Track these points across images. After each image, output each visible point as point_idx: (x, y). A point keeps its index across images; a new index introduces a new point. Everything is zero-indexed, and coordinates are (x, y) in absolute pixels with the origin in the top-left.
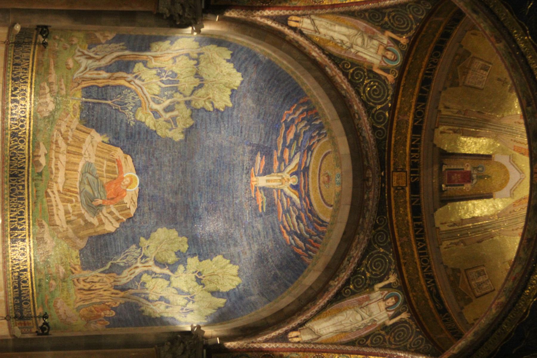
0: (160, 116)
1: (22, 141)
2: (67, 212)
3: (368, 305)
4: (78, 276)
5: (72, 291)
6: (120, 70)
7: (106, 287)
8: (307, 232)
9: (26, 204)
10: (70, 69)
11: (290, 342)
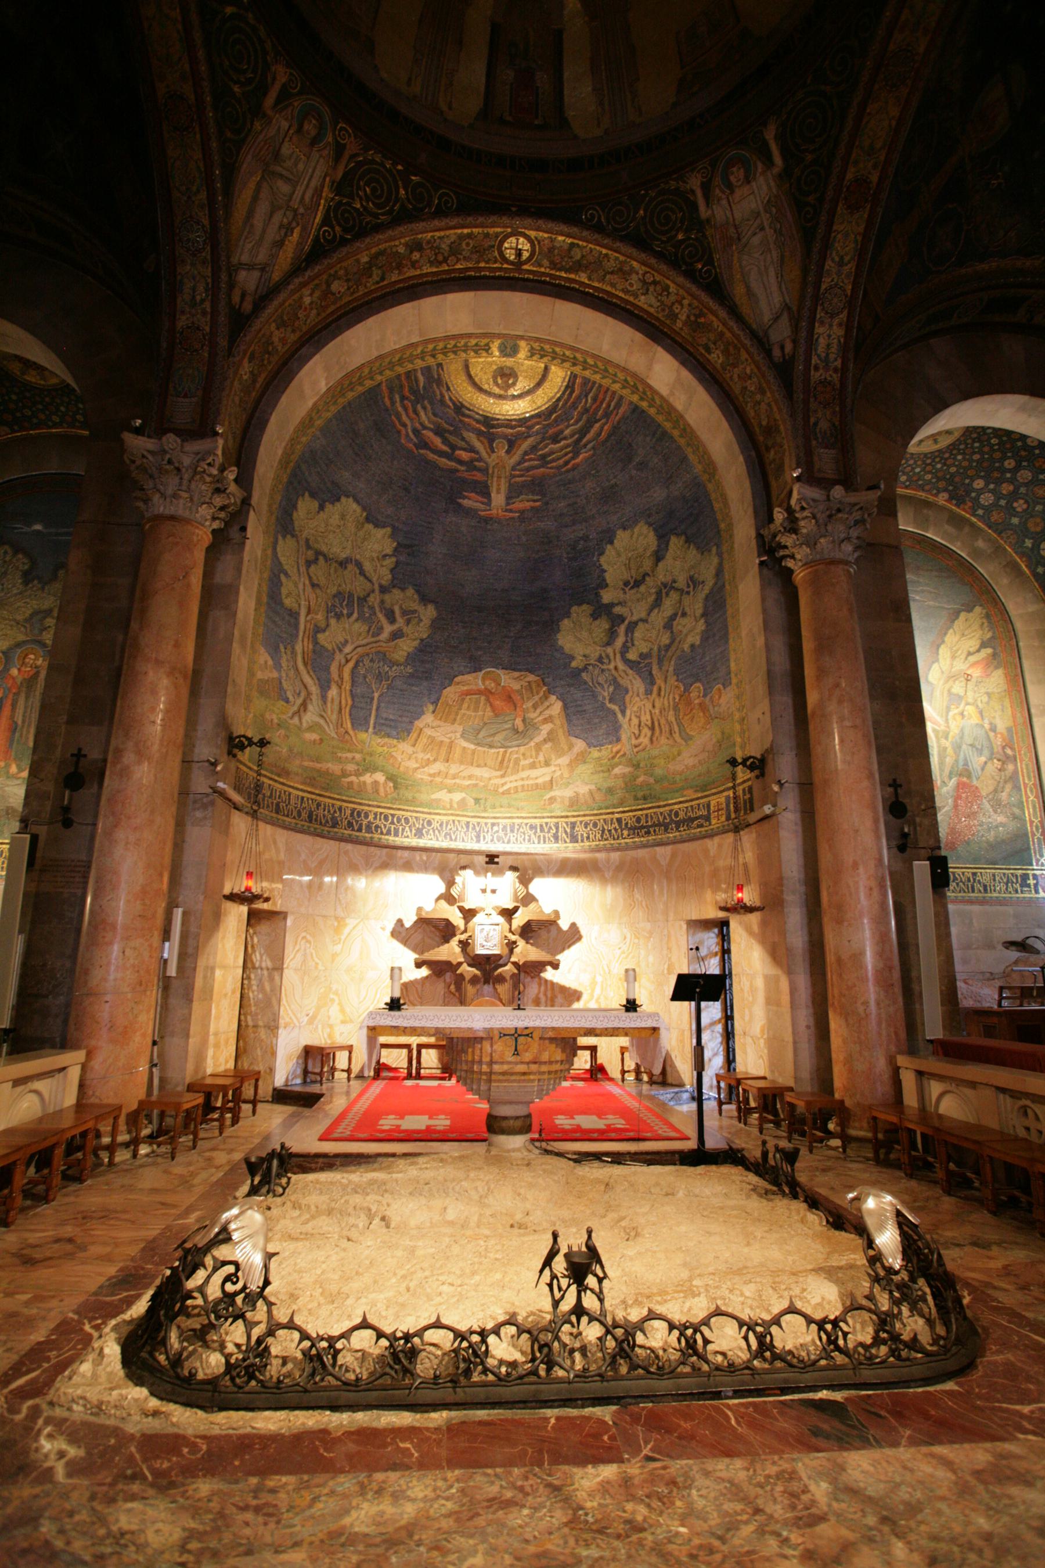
0: (400, 630)
1: (429, 823)
2: (533, 766)
3: (736, 227)
4: (628, 747)
5: (655, 752)
6: (327, 669)
7: (649, 706)
8: (577, 422)
9: (520, 821)
10: (321, 740)
11: (793, 356)
